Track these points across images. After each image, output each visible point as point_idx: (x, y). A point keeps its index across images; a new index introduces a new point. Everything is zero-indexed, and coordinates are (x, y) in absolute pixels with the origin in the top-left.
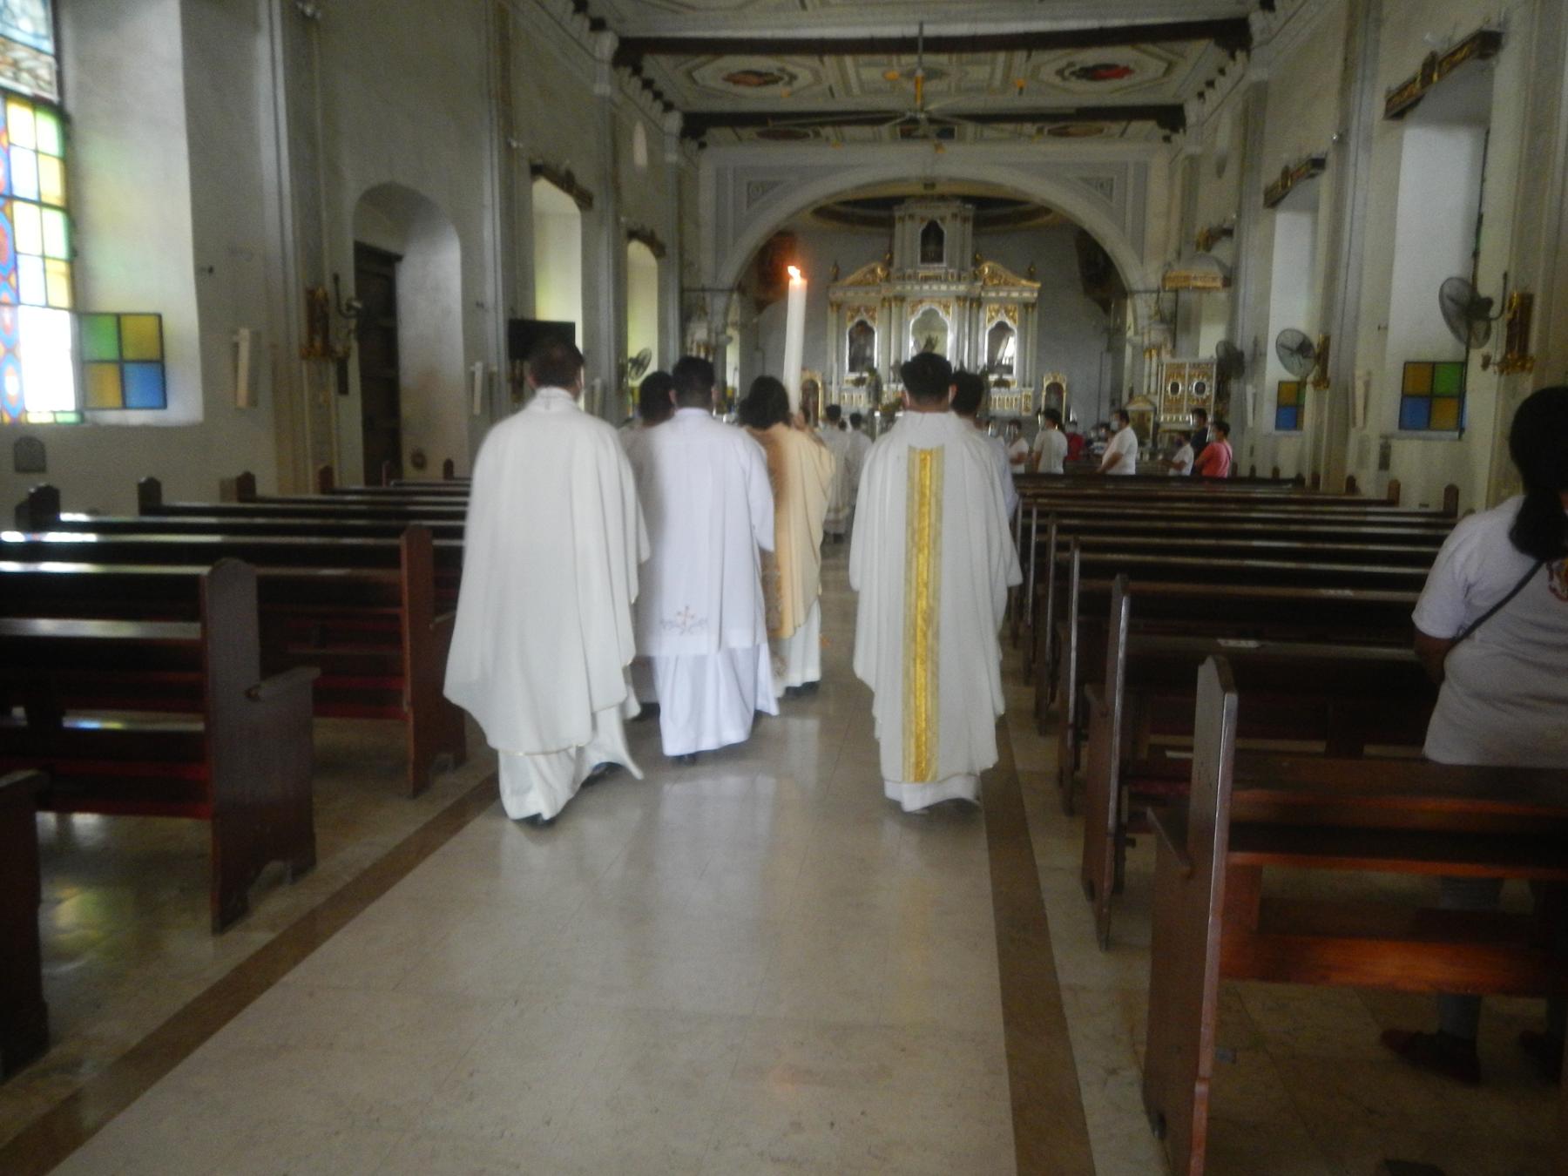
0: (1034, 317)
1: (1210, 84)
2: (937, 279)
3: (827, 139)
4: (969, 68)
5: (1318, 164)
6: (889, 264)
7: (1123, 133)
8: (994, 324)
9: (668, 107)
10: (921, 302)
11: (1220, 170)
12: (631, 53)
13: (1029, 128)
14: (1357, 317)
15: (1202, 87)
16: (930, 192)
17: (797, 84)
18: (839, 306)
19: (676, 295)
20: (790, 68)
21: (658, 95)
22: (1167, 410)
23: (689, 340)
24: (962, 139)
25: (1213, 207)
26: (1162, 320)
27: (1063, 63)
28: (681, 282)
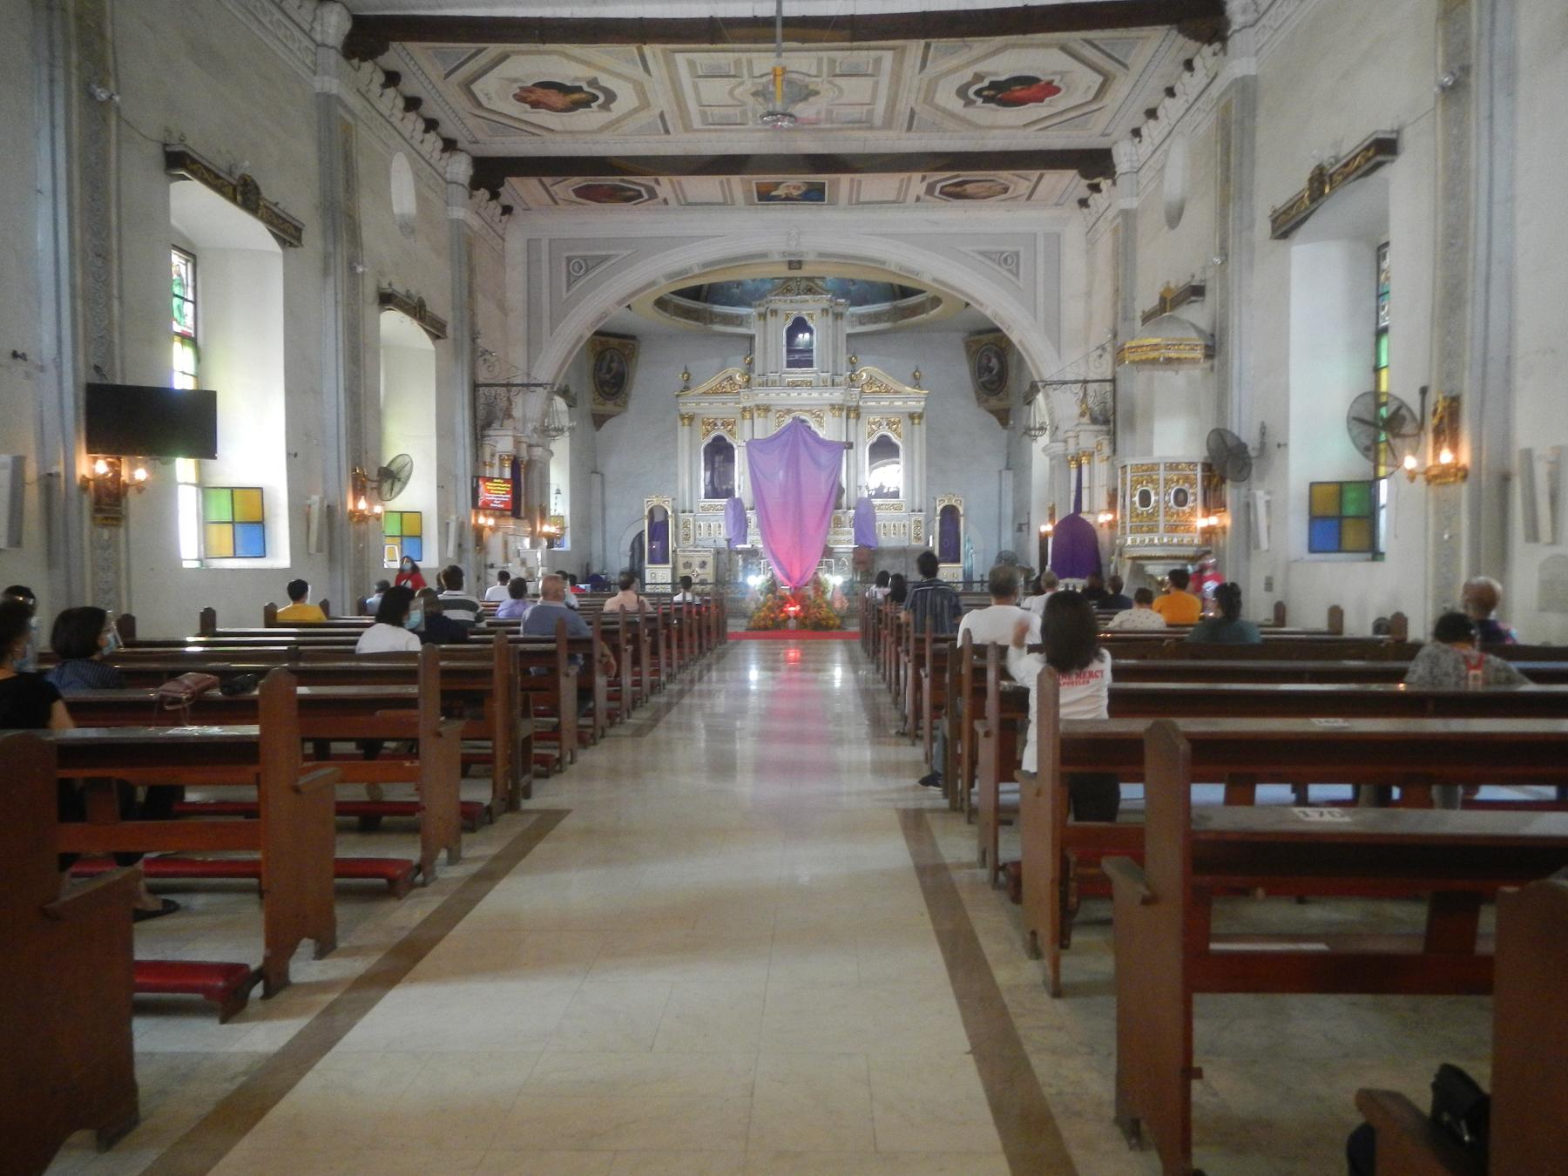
0: (920, 430)
1: (1151, 114)
2: (809, 384)
5: (1384, 148)
6: (750, 368)
8: (874, 439)
9: (450, 145)
10: (789, 411)
11: (1174, 217)
13: (916, 183)
14: (1508, 361)
15: (1138, 120)
17: (618, 108)
18: (691, 418)
20: (606, 81)
21: (431, 125)
22: (1137, 530)
23: (487, 451)
24: (833, 203)
25: (1165, 261)
26: (1094, 421)
27: (967, 75)
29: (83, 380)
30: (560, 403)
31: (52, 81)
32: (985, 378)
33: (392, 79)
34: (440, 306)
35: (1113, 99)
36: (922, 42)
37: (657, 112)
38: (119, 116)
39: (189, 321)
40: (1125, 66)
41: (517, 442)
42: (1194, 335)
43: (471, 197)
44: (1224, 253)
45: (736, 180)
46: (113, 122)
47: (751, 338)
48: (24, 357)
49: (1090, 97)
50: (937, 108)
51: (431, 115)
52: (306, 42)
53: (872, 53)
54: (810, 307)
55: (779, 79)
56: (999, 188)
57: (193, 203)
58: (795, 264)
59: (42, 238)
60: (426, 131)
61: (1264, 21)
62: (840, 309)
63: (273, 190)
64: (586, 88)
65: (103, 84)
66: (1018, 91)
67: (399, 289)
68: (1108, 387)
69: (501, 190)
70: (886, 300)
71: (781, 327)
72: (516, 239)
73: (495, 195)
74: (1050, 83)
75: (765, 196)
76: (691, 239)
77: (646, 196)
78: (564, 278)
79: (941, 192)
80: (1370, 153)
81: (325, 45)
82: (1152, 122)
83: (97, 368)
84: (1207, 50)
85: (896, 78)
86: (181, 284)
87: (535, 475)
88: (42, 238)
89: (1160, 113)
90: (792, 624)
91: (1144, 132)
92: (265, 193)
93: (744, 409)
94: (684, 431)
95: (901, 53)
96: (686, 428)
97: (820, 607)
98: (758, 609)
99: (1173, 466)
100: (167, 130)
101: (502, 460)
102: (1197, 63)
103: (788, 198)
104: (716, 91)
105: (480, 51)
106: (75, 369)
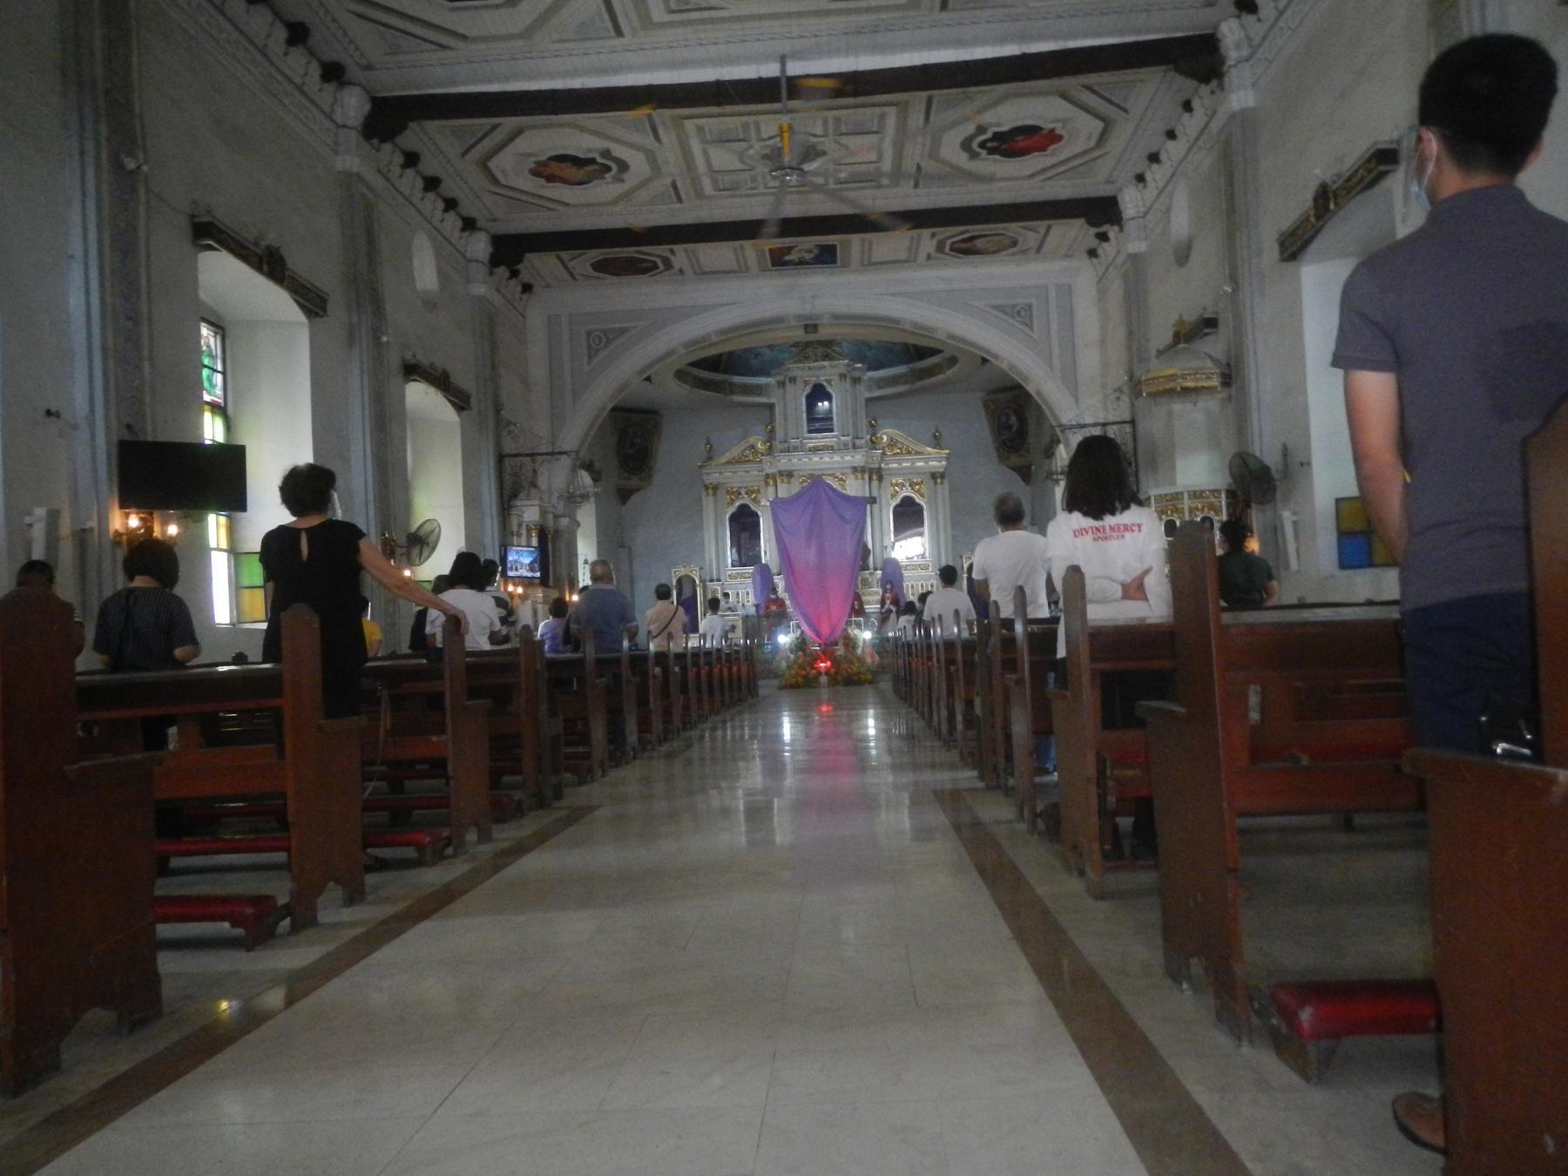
0: (944, 489)
1: (1154, 158)
3: (681, 272)
4: (850, 141)
6: (771, 437)
7: (1038, 251)
8: (898, 500)
9: (469, 224)
11: (1183, 255)
12: (389, 118)
13: (927, 240)
15: (1142, 165)
16: (812, 337)
17: (631, 179)
18: (715, 488)
19: (492, 462)
21: (451, 204)
23: (514, 521)
25: (1176, 297)
27: (970, 129)
28: (498, 443)
29: (115, 439)
30: (585, 478)
31: (82, 153)
32: (1006, 435)
33: (411, 159)
34: (464, 379)
35: (1116, 144)
36: (924, 94)
37: (668, 181)
38: (148, 190)
39: (219, 391)
40: (1126, 111)
41: (543, 512)
42: (1209, 363)
43: (491, 274)
44: (1234, 279)
45: (747, 244)
46: (142, 191)
47: (771, 407)
48: (58, 415)
49: (1092, 143)
50: (944, 162)
51: (449, 194)
52: (327, 123)
53: (878, 110)
54: (828, 372)
55: (786, 135)
56: (1008, 242)
57: (222, 274)
58: (811, 328)
59: (75, 301)
60: (446, 210)
61: (1258, 56)
62: (857, 374)
63: (297, 261)
64: (599, 160)
65: (131, 154)
66: (1021, 141)
67: (423, 359)
68: (1128, 428)
69: (520, 267)
70: (900, 363)
71: (798, 397)
72: (536, 315)
73: (514, 274)
74: (1052, 130)
75: (779, 260)
76: (707, 308)
77: (662, 267)
78: (585, 351)
79: (952, 249)
80: (1372, 165)
81: (344, 126)
82: (1155, 166)
83: (129, 426)
84: (1204, 90)
85: (902, 127)
86: (211, 356)
87: (562, 545)
88: (75, 301)
89: (1163, 156)
90: (824, 679)
91: (1148, 177)
92: (290, 264)
93: (767, 476)
94: (708, 503)
95: (904, 109)
96: (711, 499)
97: (851, 663)
98: (789, 667)
99: (1196, 495)
100: (194, 202)
101: (529, 530)
102: (1196, 104)
103: (801, 263)
104: (723, 158)
105: (494, 127)
106: (108, 427)
